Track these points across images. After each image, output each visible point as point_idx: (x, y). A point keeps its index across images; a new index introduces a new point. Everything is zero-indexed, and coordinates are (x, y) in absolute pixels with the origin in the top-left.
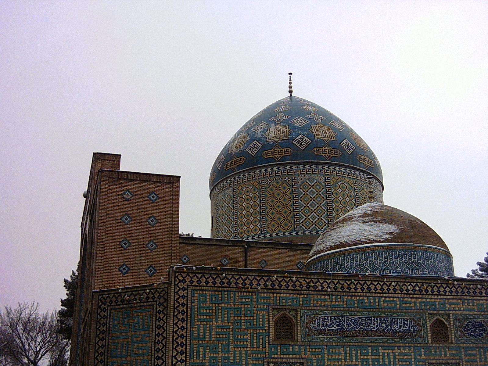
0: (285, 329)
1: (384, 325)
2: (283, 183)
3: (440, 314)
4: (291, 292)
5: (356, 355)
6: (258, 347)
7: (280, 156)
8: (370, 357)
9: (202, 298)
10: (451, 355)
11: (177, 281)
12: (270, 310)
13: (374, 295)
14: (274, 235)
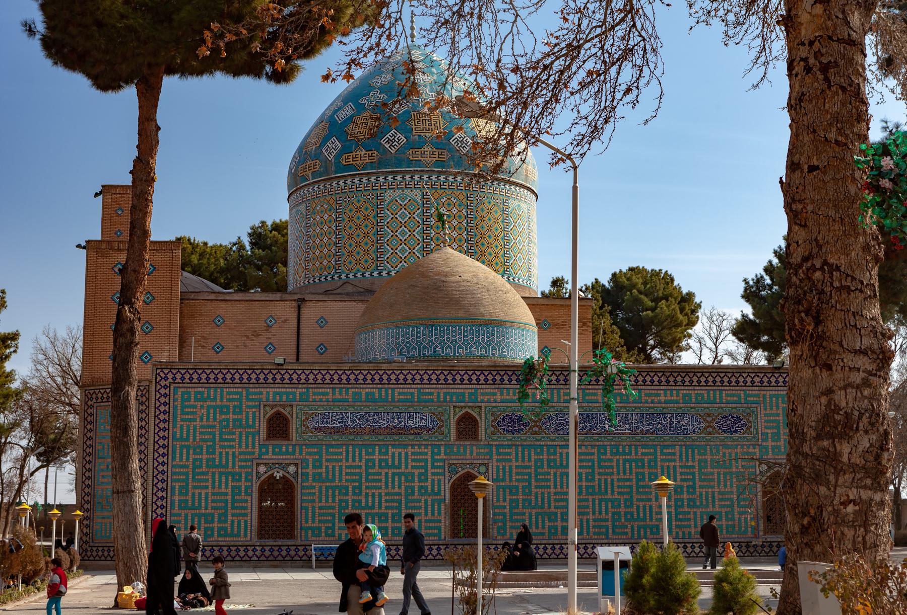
0: (278, 427)
1: (396, 421)
3: (469, 407)
4: (287, 386)
5: (360, 454)
6: (247, 447)
8: (376, 457)
9: (186, 396)
10: (478, 454)
11: (159, 378)
12: (262, 407)
13: (386, 386)
14: (351, 276)
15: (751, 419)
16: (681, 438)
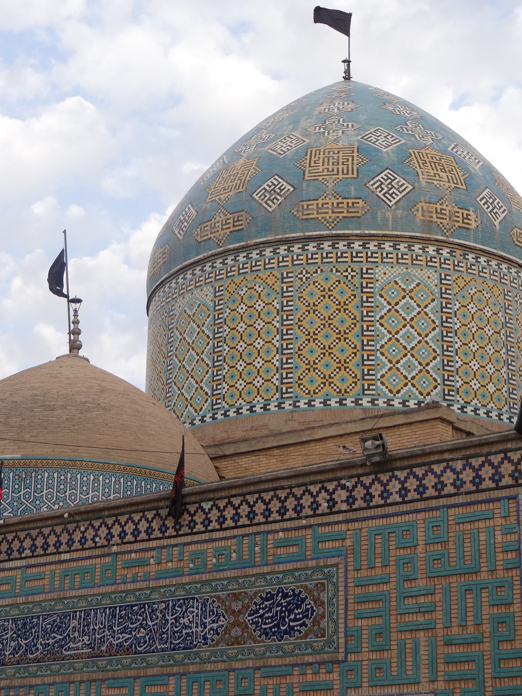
2: (339, 282)
7: (338, 217)
15: (324, 597)
16: (179, 656)
